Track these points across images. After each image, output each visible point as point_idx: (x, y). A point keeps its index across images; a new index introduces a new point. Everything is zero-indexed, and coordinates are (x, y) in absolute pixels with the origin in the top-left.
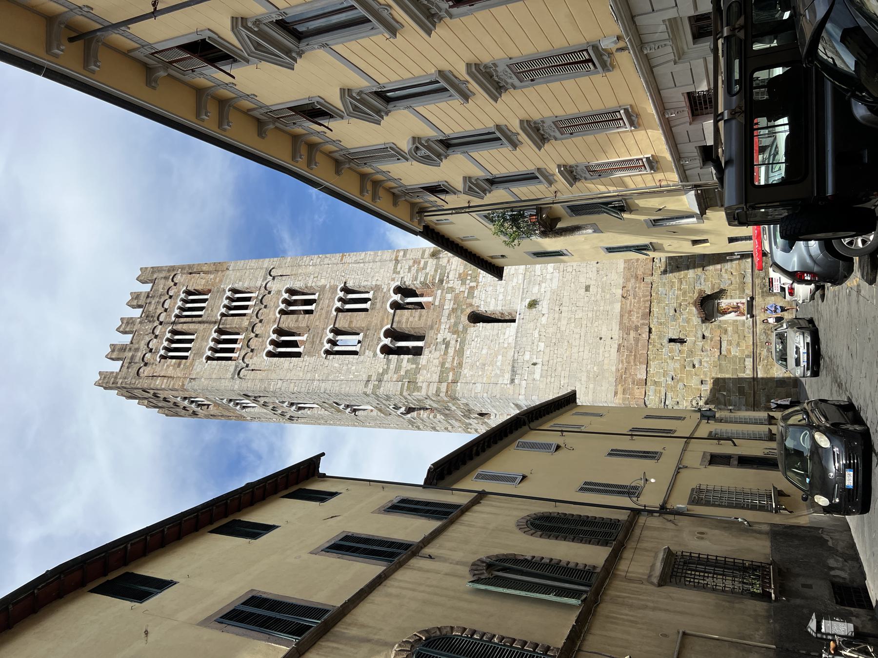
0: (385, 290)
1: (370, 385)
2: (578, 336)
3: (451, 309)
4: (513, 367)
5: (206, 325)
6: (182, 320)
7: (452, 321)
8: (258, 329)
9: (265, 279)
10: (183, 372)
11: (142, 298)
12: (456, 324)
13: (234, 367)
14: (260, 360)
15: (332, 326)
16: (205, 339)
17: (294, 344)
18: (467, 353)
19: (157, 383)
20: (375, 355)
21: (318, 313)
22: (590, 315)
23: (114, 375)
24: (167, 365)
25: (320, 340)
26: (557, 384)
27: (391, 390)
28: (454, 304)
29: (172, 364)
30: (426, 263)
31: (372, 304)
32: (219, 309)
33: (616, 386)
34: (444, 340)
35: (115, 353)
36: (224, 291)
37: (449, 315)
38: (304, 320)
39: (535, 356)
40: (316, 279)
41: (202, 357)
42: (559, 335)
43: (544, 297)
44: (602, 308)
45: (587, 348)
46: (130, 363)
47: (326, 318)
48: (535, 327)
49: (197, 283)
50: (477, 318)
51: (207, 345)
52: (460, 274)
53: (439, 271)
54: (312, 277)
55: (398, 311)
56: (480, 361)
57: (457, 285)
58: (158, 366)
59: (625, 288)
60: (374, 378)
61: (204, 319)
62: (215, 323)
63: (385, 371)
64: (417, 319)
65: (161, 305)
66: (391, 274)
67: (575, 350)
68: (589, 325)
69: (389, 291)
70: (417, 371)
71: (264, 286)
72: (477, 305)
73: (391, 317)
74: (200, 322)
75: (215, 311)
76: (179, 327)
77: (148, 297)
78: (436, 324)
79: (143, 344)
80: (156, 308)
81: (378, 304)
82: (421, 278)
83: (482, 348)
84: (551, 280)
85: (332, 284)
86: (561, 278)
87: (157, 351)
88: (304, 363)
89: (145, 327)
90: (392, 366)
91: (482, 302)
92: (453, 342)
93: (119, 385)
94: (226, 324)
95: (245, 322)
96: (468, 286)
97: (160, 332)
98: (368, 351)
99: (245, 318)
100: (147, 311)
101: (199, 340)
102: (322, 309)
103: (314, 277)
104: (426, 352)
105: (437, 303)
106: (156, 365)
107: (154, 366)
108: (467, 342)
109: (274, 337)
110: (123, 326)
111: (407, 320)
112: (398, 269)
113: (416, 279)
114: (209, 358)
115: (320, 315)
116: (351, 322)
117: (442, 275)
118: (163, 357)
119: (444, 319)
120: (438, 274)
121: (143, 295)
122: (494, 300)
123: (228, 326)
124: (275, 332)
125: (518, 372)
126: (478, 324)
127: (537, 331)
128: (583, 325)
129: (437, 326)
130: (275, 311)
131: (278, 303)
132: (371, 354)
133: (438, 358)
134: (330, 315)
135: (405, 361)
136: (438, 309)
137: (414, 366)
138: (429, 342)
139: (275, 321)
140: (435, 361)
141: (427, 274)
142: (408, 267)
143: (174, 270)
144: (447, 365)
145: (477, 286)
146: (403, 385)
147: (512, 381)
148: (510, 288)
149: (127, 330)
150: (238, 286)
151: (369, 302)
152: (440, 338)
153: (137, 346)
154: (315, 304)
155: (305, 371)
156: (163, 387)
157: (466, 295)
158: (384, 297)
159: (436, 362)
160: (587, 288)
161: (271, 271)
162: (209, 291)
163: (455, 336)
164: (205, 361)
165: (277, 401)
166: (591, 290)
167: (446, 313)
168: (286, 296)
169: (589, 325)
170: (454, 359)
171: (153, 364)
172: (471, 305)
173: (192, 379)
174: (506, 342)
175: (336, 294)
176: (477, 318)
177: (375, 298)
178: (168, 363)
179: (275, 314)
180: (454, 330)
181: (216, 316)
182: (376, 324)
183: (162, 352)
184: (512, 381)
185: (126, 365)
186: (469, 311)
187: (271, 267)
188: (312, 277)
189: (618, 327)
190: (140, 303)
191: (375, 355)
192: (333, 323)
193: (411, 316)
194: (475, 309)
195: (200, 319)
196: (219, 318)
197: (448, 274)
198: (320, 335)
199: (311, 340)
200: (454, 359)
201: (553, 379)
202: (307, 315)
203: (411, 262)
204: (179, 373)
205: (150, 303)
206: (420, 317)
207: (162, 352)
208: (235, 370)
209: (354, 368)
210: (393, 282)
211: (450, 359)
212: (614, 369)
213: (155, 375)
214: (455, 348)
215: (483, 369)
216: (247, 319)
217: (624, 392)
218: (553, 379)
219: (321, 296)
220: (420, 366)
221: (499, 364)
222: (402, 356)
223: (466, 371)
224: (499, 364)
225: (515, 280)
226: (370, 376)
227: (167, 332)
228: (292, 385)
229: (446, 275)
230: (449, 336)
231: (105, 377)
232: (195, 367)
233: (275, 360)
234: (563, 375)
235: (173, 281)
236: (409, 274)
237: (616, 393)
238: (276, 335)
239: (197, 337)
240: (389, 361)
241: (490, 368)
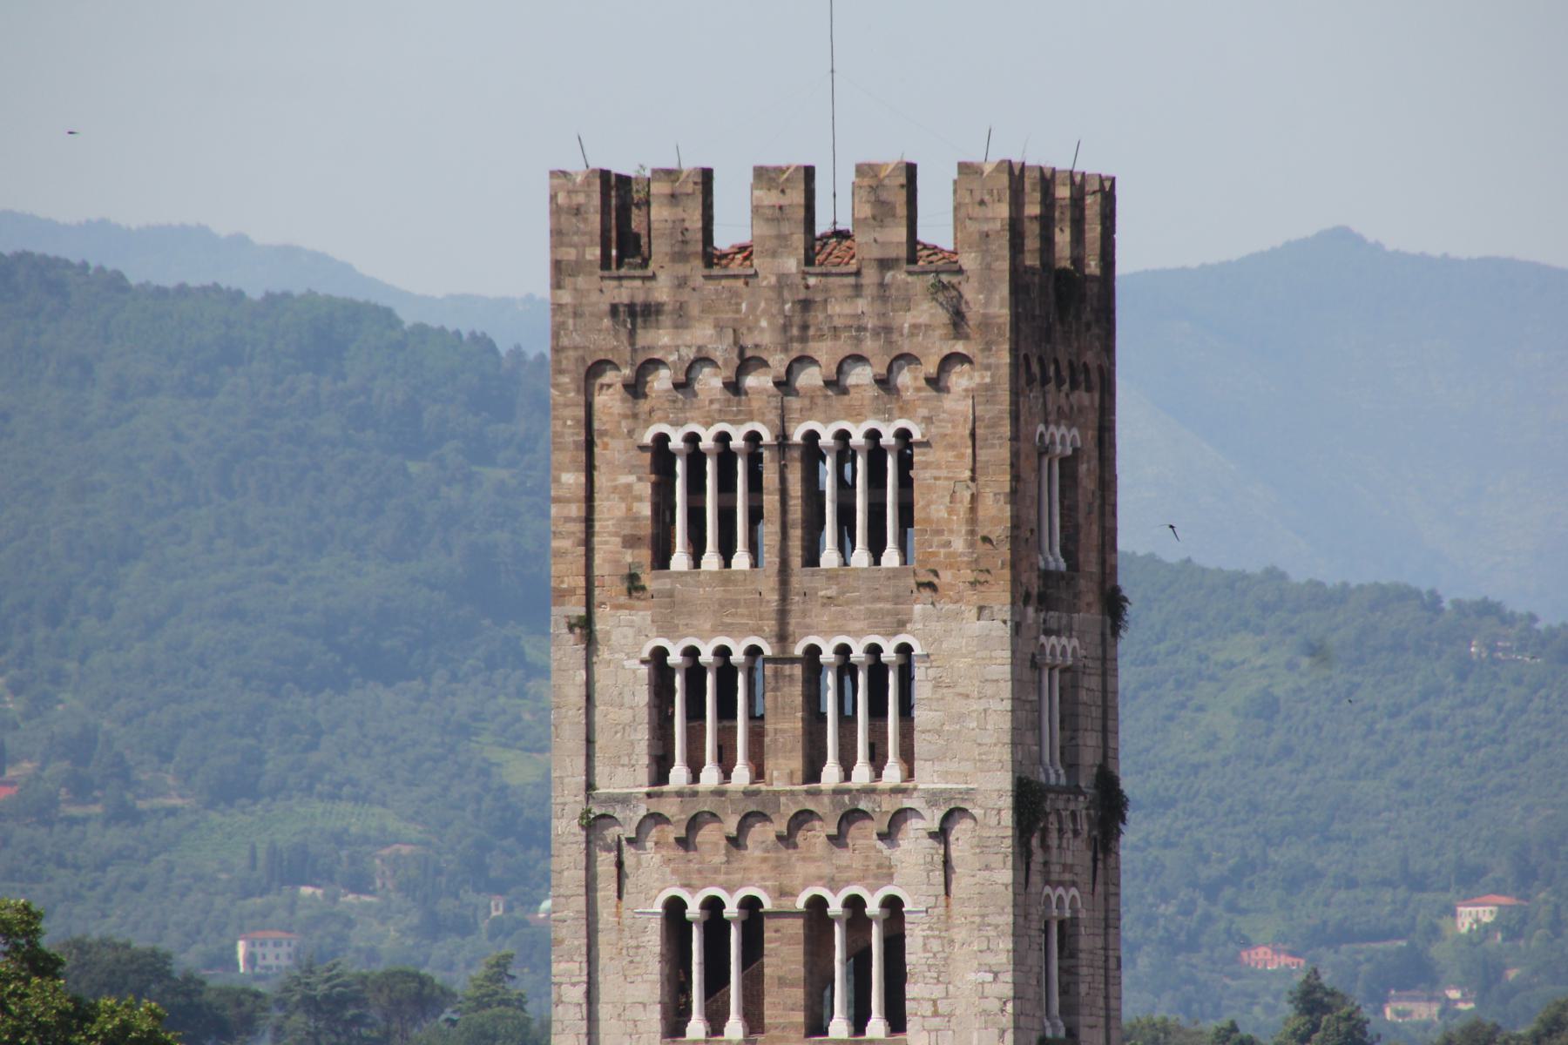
5: (775, 597)
29: (636, 506)
36: (901, 625)
51: (700, 637)
61: (800, 577)
79: (702, 334)
100: (826, 290)
107: (625, 426)
188: (938, 992)
232: (624, 615)
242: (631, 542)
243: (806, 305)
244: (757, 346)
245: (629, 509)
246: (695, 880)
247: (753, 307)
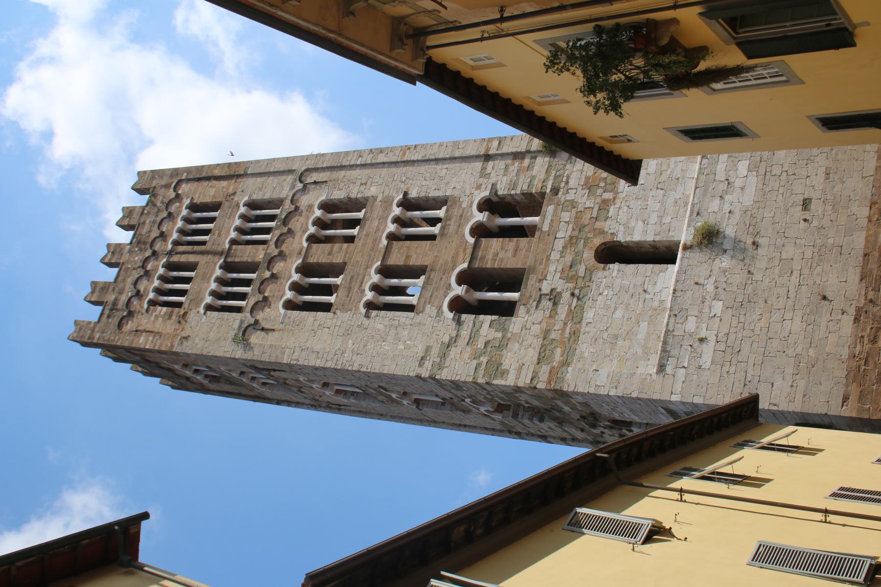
0: (464, 205)
1: (427, 363)
2: (782, 292)
3: (567, 239)
4: (665, 343)
6: (181, 248)
7: (568, 259)
9: (293, 187)
10: (174, 327)
11: (134, 216)
13: (238, 322)
15: (379, 263)
16: (206, 278)
17: (328, 290)
18: (589, 315)
19: (141, 341)
21: (362, 241)
22: (809, 253)
23: (92, 325)
24: (156, 316)
25: (361, 286)
26: (740, 375)
27: (459, 373)
28: (573, 229)
29: (162, 314)
31: (443, 228)
32: (228, 233)
33: (847, 385)
34: (552, 290)
35: (95, 295)
36: (238, 205)
37: (564, 247)
39: (704, 326)
40: (363, 187)
41: (199, 307)
42: (750, 289)
43: (729, 218)
44: (831, 241)
45: (799, 313)
46: (111, 310)
47: (372, 249)
48: (708, 273)
49: (207, 193)
52: (587, 178)
53: (554, 172)
54: (358, 183)
55: (484, 241)
56: (610, 330)
57: (584, 201)
58: (144, 315)
59: (877, 206)
60: (435, 351)
61: (207, 247)
62: (221, 253)
63: (454, 341)
64: (510, 254)
65: (156, 225)
66: (477, 179)
67: (777, 316)
68: (806, 271)
69: (471, 206)
71: (290, 198)
72: (612, 231)
73: (469, 251)
74: (202, 253)
75: (223, 236)
76: (175, 259)
77: (142, 213)
78: (541, 264)
80: (150, 231)
81: (451, 227)
82: (522, 186)
83: (616, 309)
84: (742, 189)
85: (386, 194)
86: (760, 186)
88: (335, 320)
89: (134, 258)
90: (465, 333)
91: (622, 228)
92: (566, 296)
93: (95, 341)
94: (235, 257)
95: (259, 254)
96: (599, 200)
97: (151, 266)
98: (429, 306)
99: (261, 247)
100: (139, 235)
101: (198, 280)
102: (367, 235)
103: (362, 184)
104: (521, 310)
105: (545, 228)
106: (142, 314)
108: (590, 295)
109: (296, 277)
110: (109, 257)
112: (488, 171)
113: (514, 186)
114: (209, 308)
115: (364, 245)
116: (408, 257)
118: (152, 303)
119: (555, 256)
120: (551, 178)
121: (137, 210)
122: (640, 223)
123: (237, 260)
124: (298, 270)
125: (673, 353)
126: (611, 266)
127: (712, 280)
128: (794, 272)
129: (542, 267)
130: (301, 237)
131: (307, 224)
133: (540, 323)
134: (378, 245)
135: (486, 325)
136: (546, 237)
137: (499, 335)
138: (527, 295)
139: (300, 253)
140: (534, 327)
141: (533, 178)
142: (504, 167)
143: (177, 175)
144: (553, 335)
145: (614, 198)
146: (479, 365)
148: (670, 201)
149: (113, 261)
150: (258, 196)
151: (439, 225)
152: (546, 288)
153: (121, 285)
154: (359, 226)
155: (335, 334)
156: (147, 347)
157: (595, 215)
158: (462, 216)
159: (536, 329)
160: (806, 204)
161: (302, 174)
162: (216, 207)
163: (571, 285)
164: (202, 311)
165: (301, 379)
166: (813, 207)
167: (559, 245)
168: (318, 213)
169: (806, 271)
170: (565, 324)
171: (139, 312)
172: (602, 232)
173: (184, 338)
174: (657, 299)
175: (391, 210)
177: (448, 218)
178: (157, 313)
179: (301, 243)
180: (569, 274)
181: (224, 243)
182: (446, 262)
183: (151, 295)
184: (661, 368)
185: (107, 312)
186: (597, 242)
187: (303, 169)
189: (858, 277)
190: (132, 223)
192: (381, 258)
193: (502, 248)
194: (608, 239)
195: (203, 248)
196: (227, 246)
197: (568, 177)
198: (360, 277)
199: (347, 285)
200: (565, 324)
201: (733, 369)
202: (346, 245)
204: (169, 327)
205: (144, 223)
207: (151, 295)
208: (240, 327)
209: (406, 333)
210: (478, 191)
212: (845, 353)
213: (140, 328)
214: (570, 306)
215: (613, 345)
216: (263, 250)
217: (861, 397)
218: (733, 369)
219: (368, 215)
220: (509, 335)
221: (641, 336)
222: (482, 317)
223: (584, 348)
224: (641, 336)
225: (680, 188)
227: (160, 266)
228: (314, 356)
229: (565, 179)
231: (80, 329)
233: (296, 313)
234: (751, 362)
235: (175, 190)
236: (505, 178)
237: (845, 399)
238: (299, 275)
239: (196, 276)
240: (459, 323)
241: (627, 343)
244: (141, 261)
245: (161, 316)
246: (281, 293)
247: (131, 262)
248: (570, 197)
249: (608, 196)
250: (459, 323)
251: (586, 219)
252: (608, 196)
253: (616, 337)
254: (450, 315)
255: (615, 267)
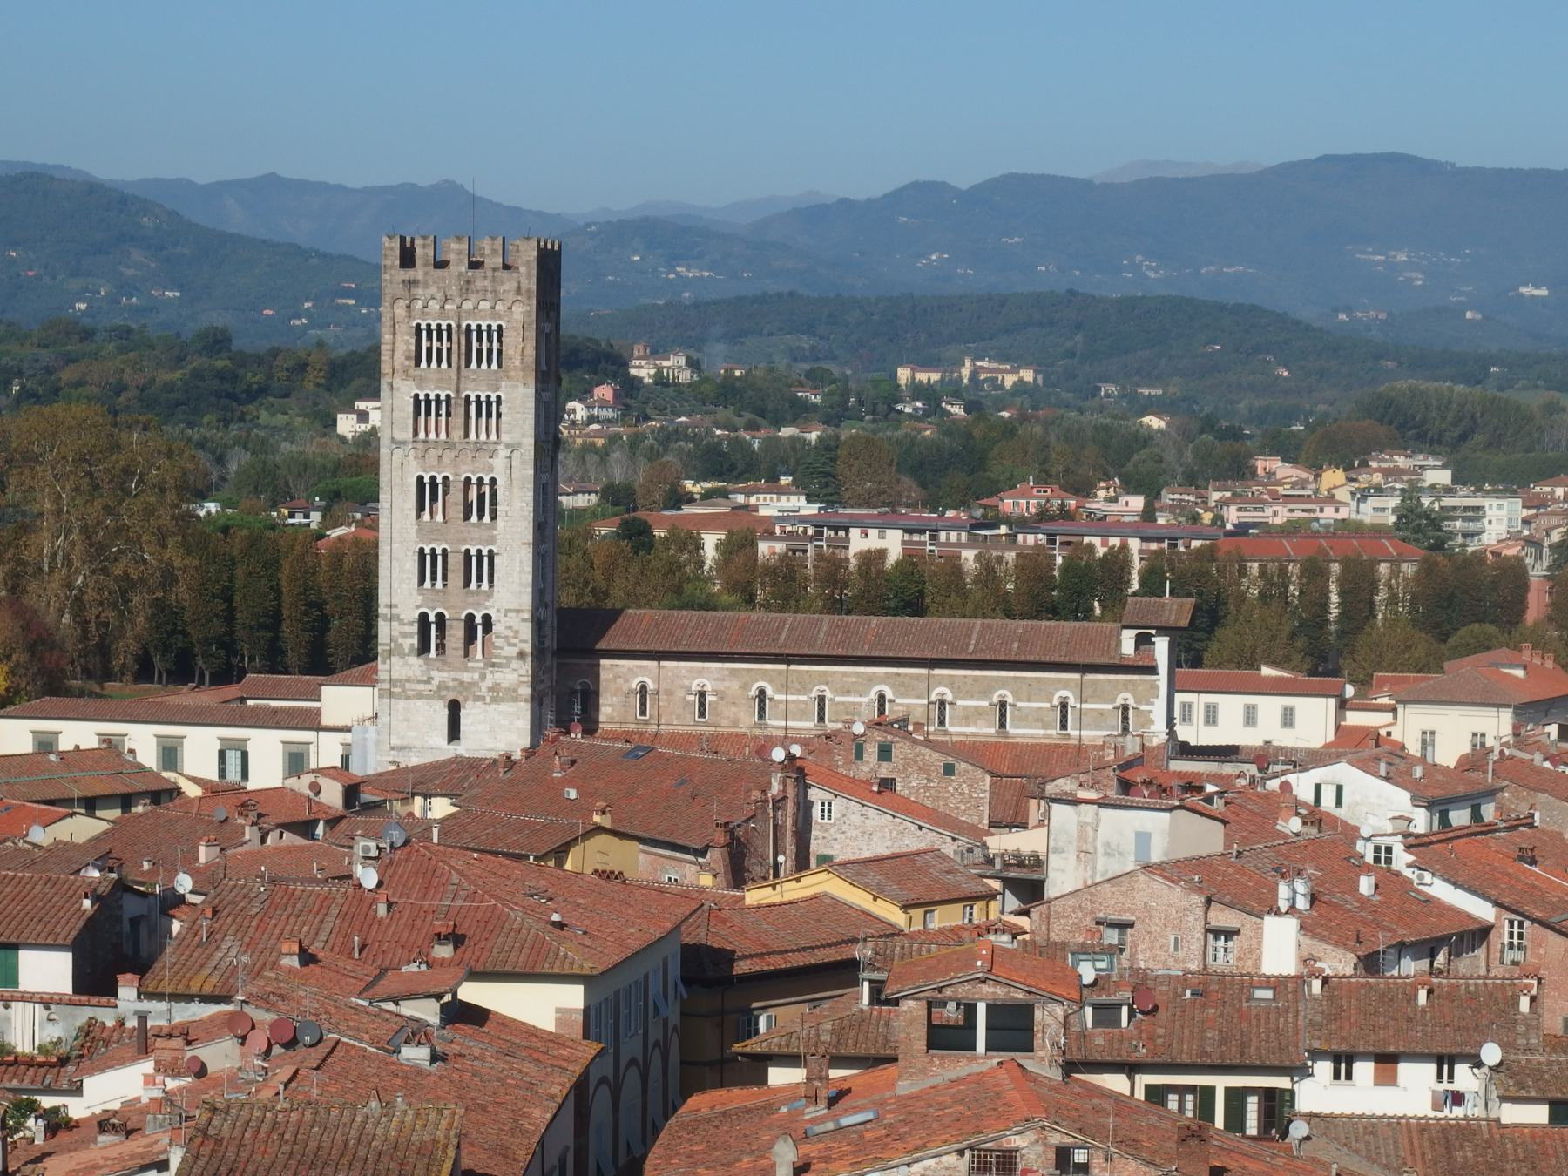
7: (451, 684)
8: (448, 456)
12: (447, 688)
14: (413, 471)
18: (419, 703)
20: (418, 607)
30: (515, 645)
38: (456, 511)
50: (454, 708)
54: (507, 508)
57: (488, 683)
62: (458, 391)
63: (402, 623)
64: (454, 645)
70: (402, 655)
75: (472, 385)
87: (424, 315)
90: (407, 629)
92: (429, 687)
105: (470, 665)
111: (456, 634)
112: (509, 614)
117: (499, 665)
119: (453, 675)
130: (469, 471)
132: (418, 603)
141: (502, 648)
144: (407, 685)
147: (392, 749)
159: (411, 674)
167: (459, 675)
176: (454, 708)
180: (442, 686)
186: (460, 699)
188: (507, 508)
191: (418, 607)
195: (463, 366)
203: (515, 628)
204: (400, 358)
206: (456, 649)
211: (413, 686)
221: (410, 734)
226: (396, 606)
230: (435, 682)
240: (411, 624)
242: (408, 358)
243: (468, 282)
248: (489, 676)
249: (488, 700)
250: (411, 624)
251: (475, 689)
252: (488, 700)
253: (408, 720)
254: (417, 616)
255: (446, 712)
